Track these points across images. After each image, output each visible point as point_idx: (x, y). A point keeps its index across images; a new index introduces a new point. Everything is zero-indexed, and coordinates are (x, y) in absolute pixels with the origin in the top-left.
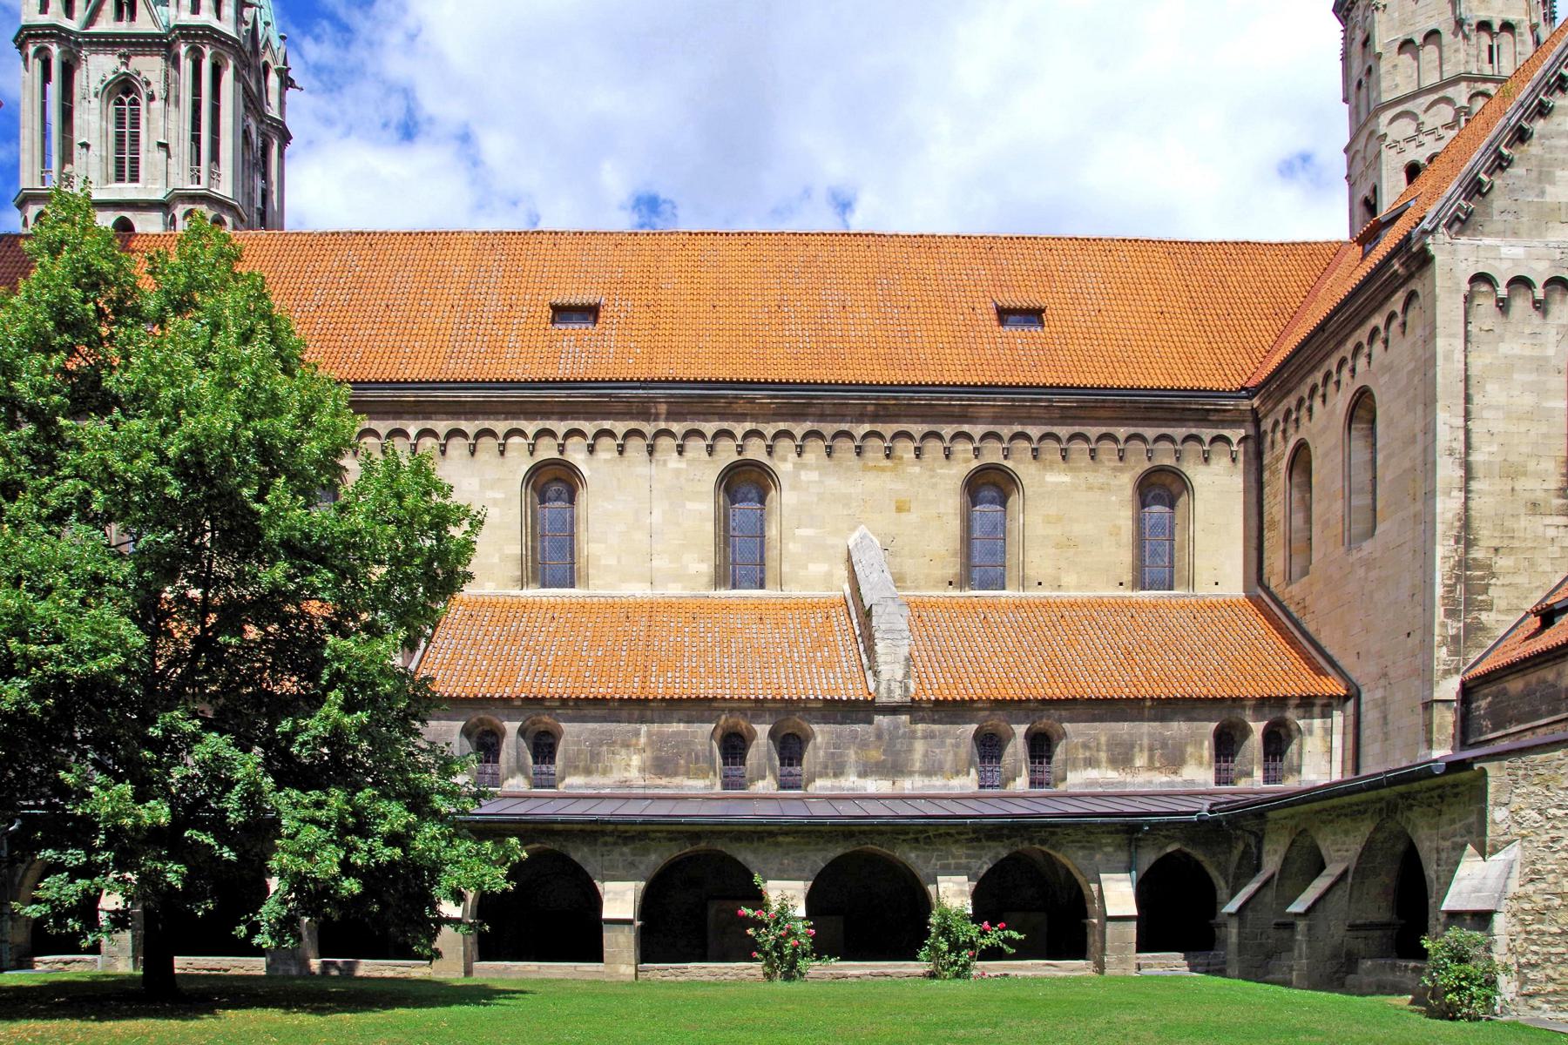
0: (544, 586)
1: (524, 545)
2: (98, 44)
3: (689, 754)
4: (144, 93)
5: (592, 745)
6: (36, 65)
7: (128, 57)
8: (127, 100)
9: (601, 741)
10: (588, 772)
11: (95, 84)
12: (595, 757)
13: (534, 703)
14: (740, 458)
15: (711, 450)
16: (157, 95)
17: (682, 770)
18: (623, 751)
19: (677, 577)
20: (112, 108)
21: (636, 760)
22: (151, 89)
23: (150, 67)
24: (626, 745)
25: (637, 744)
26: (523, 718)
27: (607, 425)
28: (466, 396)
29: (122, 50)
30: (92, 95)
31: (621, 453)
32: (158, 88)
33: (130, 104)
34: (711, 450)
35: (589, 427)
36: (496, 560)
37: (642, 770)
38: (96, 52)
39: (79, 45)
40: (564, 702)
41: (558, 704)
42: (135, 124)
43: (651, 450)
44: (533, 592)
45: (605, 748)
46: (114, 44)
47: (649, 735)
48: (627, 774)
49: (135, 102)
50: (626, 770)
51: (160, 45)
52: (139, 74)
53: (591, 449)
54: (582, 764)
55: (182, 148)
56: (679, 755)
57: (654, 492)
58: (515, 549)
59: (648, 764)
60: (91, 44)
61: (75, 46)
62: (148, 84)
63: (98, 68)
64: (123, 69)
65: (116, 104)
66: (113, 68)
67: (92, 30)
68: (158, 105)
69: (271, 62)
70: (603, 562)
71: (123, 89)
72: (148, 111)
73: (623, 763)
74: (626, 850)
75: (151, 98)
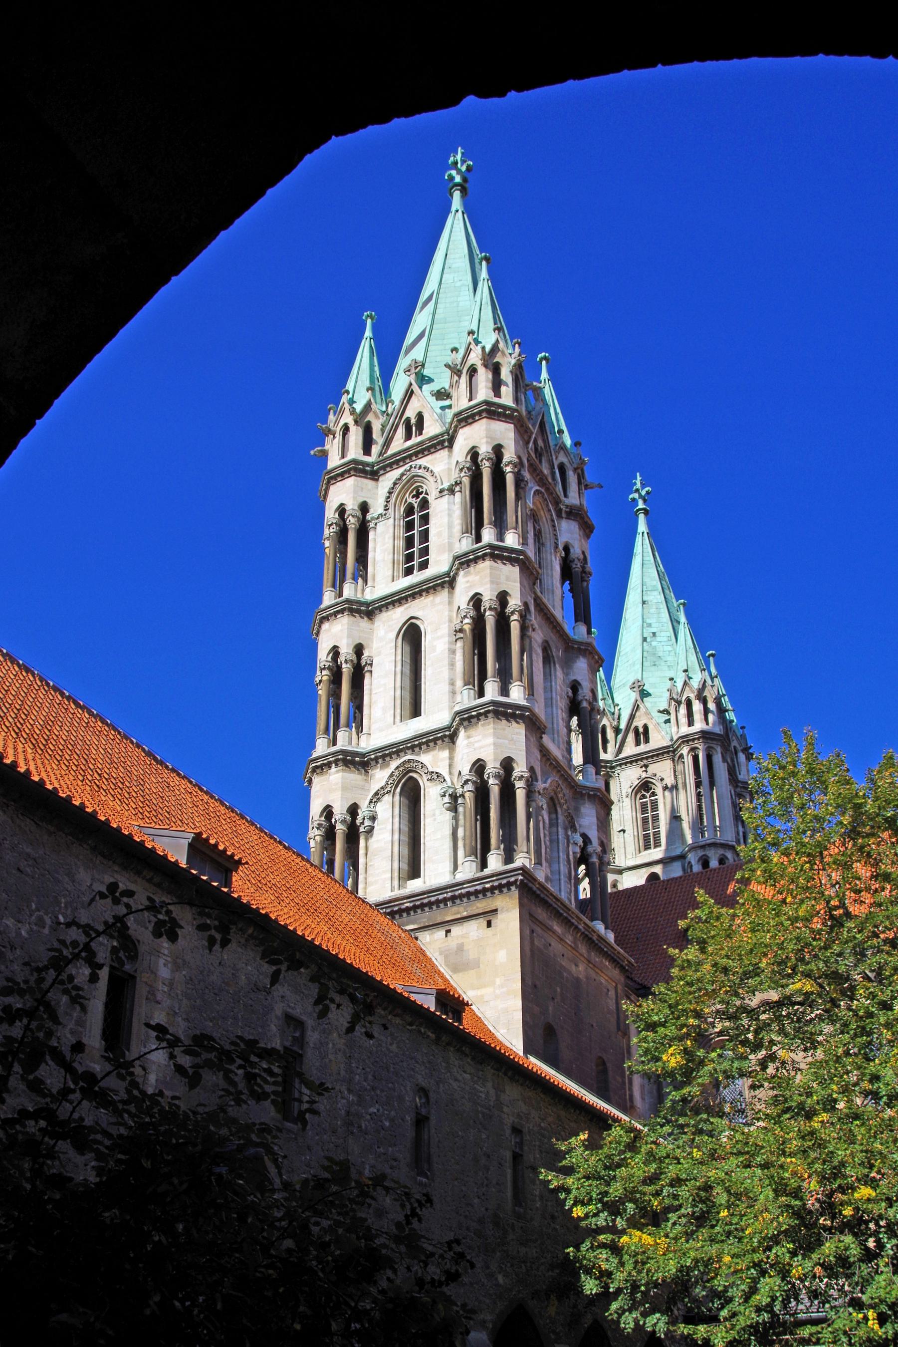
2: (626, 764)
7: (646, 766)
8: (648, 795)
22: (664, 782)
23: (663, 769)
30: (624, 796)
46: (636, 761)
52: (655, 775)
60: (621, 765)
62: (662, 780)
64: (644, 775)
66: (638, 776)
67: (621, 756)
71: (645, 786)
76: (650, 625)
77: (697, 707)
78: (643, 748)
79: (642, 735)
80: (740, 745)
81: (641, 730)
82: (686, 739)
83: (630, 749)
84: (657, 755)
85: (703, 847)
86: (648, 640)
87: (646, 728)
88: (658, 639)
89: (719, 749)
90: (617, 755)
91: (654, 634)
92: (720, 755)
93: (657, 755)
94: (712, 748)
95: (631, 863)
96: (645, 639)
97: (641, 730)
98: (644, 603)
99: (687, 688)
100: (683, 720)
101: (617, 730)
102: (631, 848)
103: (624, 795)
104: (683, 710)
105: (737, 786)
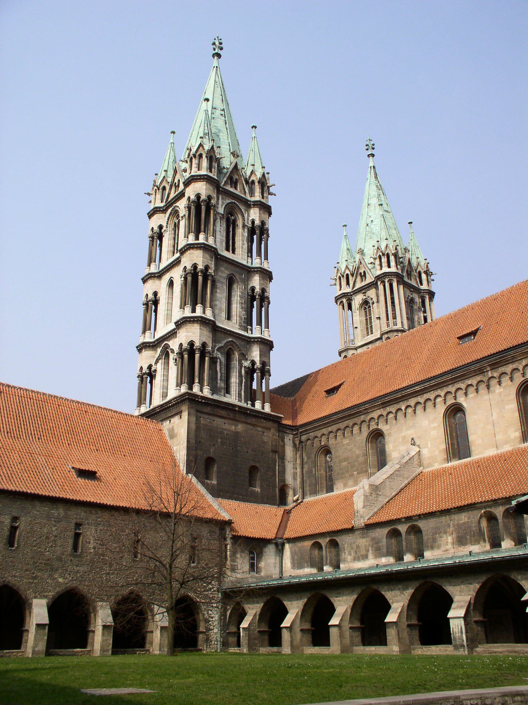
0: (460, 459)
1: (447, 443)
3: (471, 533)
4: (371, 302)
5: (432, 534)
6: (341, 306)
7: (365, 293)
9: (436, 532)
10: (432, 548)
11: (357, 306)
12: (434, 540)
13: (408, 519)
14: (524, 379)
15: (511, 379)
16: (375, 302)
17: (468, 541)
18: (445, 536)
19: (506, 442)
20: (363, 311)
21: (450, 539)
23: (371, 293)
24: (445, 533)
25: (450, 531)
26: (407, 527)
27: (469, 382)
28: (417, 388)
29: (363, 291)
31: (477, 392)
32: (375, 300)
33: (368, 308)
34: (511, 379)
35: (463, 386)
36: (437, 453)
37: (453, 543)
38: (356, 296)
39: (352, 295)
40: (420, 517)
41: (417, 517)
42: (370, 314)
43: (488, 387)
44: (456, 463)
45: (438, 535)
47: (454, 526)
48: (447, 547)
49: (370, 307)
50: (447, 545)
51: (373, 285)
53: (466, 394)
54: (429, 545)
55: (384, 316)
56: (466, 533)
57: (492, 405)
58: (443, 446)
59: (455, 540)
60: (354, 294)
61: (349, 297)
62: (372, 299)
63: (358, 300)
64: (364, 297)
65: (364, 310)
66: (361, 298)
67: (355, 289)
68: (375, 305)
69: (421, 270)
70: (477, 443)
71: (366, 303)
72: (373, 308)
73: (445, 542)
74: (400, 586)
75: (373, 303)
76: (370, 217)
77: (384, 260)
78: (364, 284)
79: (363, 276)
80: (422, 269)
81: (363, 274)
82: (378, 278)
83: (359, 285)
84: (368, 287)
85: (387, 333)
86: (369, 225)
87: (364, 272)
88: (374, 223)
89: (395, 280)
90: (353, 288)
91: (372, 221)
92: (396, 283)
93: (368, 287)
94: (392, 280)
95: (360, 344)
96: (367, 225)
97: (363, 274)
98: (369, 205)
99: (379, 251)
100: (379, 267)
101: (352, 275)
102: (360, 337)
103: (356, 309)
104: (377, 262)
105: (420, 292)
